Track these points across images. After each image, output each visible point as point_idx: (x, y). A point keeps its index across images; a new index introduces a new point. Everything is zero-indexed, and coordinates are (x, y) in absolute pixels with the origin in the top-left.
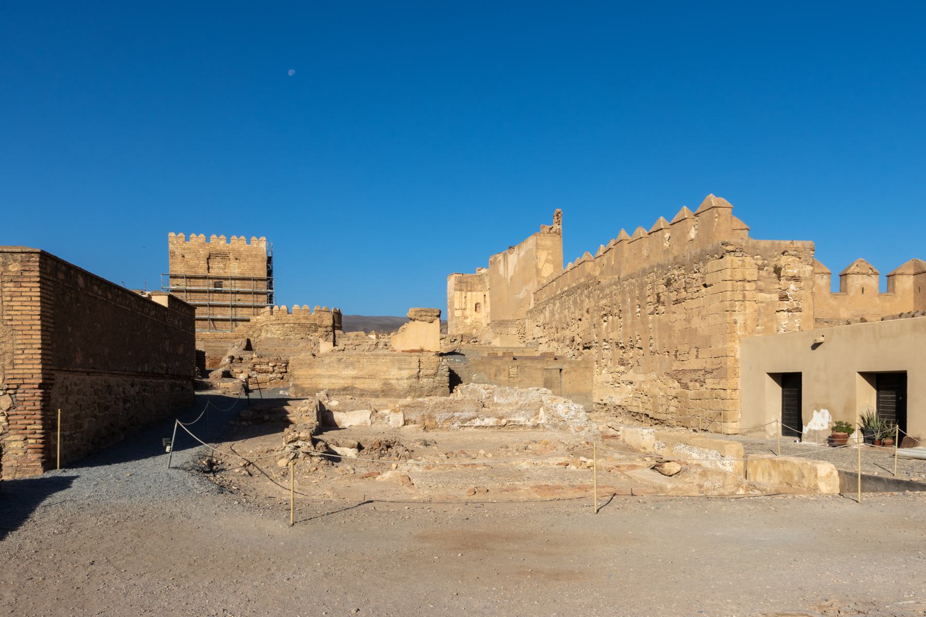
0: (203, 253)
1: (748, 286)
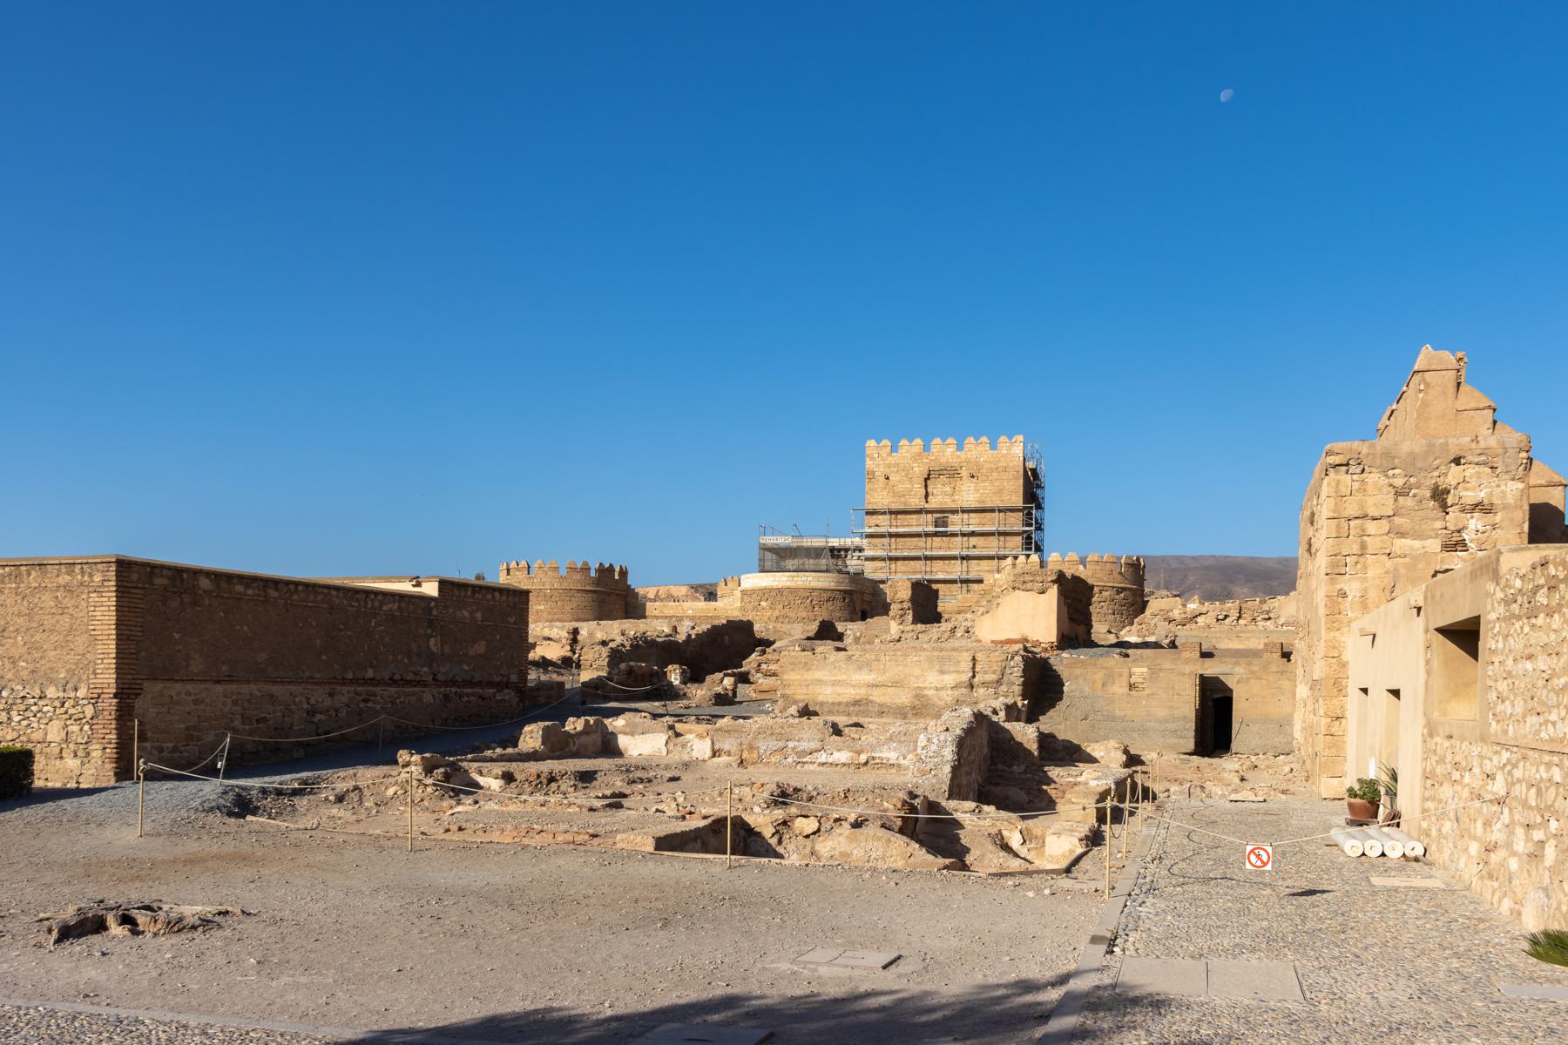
0: (919, 470)
1: (1372, 527)
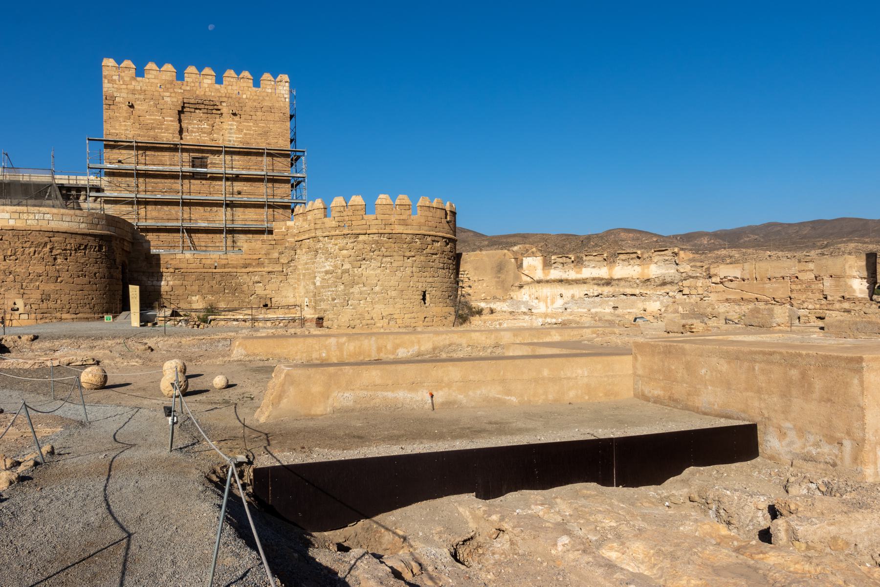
0: (171, 100)
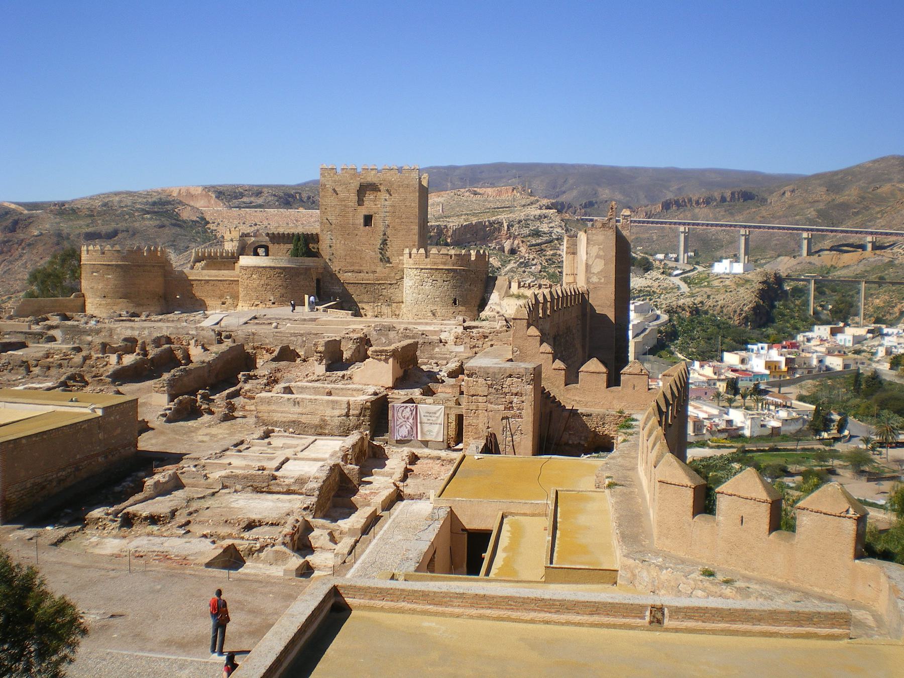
1: (480, 399)
